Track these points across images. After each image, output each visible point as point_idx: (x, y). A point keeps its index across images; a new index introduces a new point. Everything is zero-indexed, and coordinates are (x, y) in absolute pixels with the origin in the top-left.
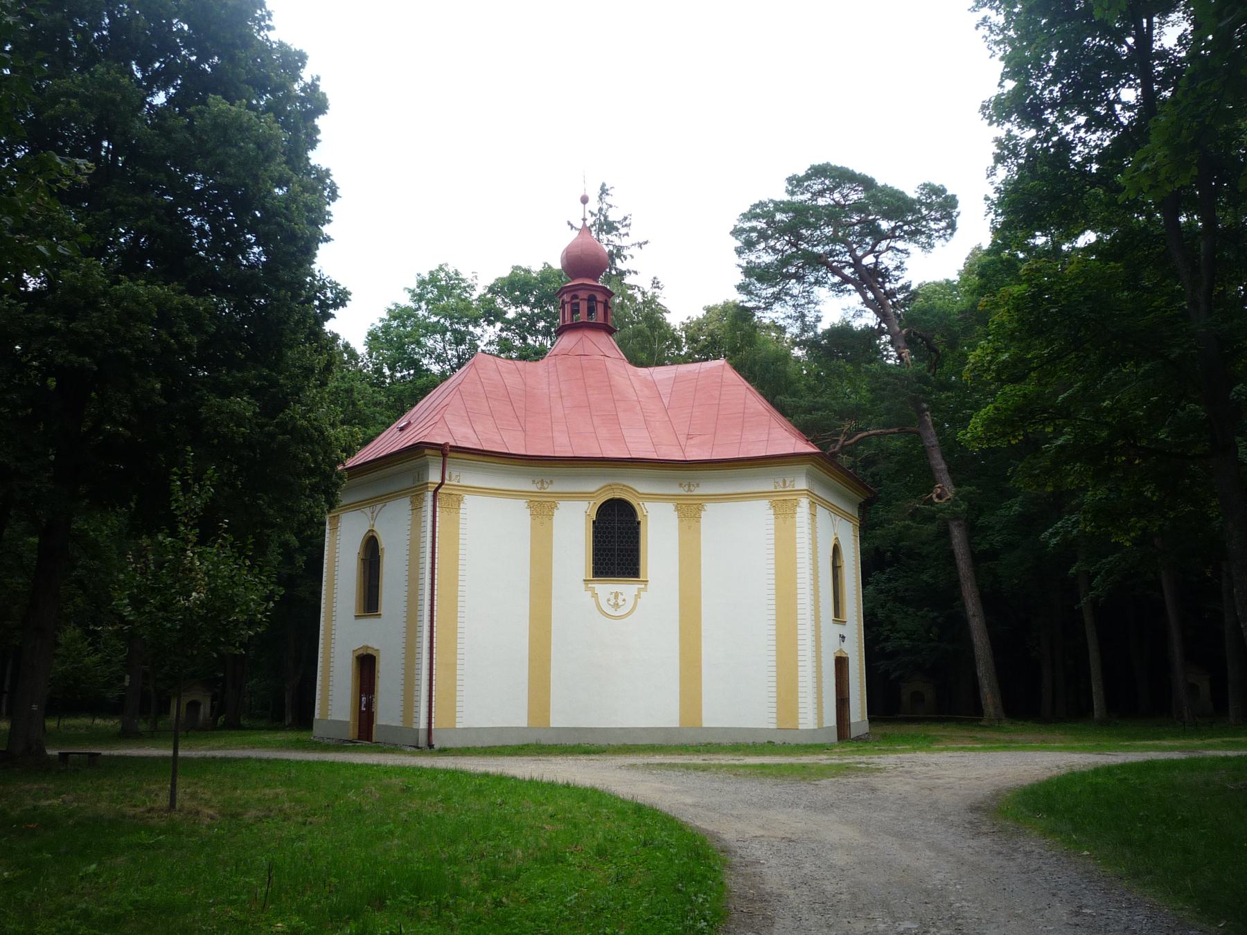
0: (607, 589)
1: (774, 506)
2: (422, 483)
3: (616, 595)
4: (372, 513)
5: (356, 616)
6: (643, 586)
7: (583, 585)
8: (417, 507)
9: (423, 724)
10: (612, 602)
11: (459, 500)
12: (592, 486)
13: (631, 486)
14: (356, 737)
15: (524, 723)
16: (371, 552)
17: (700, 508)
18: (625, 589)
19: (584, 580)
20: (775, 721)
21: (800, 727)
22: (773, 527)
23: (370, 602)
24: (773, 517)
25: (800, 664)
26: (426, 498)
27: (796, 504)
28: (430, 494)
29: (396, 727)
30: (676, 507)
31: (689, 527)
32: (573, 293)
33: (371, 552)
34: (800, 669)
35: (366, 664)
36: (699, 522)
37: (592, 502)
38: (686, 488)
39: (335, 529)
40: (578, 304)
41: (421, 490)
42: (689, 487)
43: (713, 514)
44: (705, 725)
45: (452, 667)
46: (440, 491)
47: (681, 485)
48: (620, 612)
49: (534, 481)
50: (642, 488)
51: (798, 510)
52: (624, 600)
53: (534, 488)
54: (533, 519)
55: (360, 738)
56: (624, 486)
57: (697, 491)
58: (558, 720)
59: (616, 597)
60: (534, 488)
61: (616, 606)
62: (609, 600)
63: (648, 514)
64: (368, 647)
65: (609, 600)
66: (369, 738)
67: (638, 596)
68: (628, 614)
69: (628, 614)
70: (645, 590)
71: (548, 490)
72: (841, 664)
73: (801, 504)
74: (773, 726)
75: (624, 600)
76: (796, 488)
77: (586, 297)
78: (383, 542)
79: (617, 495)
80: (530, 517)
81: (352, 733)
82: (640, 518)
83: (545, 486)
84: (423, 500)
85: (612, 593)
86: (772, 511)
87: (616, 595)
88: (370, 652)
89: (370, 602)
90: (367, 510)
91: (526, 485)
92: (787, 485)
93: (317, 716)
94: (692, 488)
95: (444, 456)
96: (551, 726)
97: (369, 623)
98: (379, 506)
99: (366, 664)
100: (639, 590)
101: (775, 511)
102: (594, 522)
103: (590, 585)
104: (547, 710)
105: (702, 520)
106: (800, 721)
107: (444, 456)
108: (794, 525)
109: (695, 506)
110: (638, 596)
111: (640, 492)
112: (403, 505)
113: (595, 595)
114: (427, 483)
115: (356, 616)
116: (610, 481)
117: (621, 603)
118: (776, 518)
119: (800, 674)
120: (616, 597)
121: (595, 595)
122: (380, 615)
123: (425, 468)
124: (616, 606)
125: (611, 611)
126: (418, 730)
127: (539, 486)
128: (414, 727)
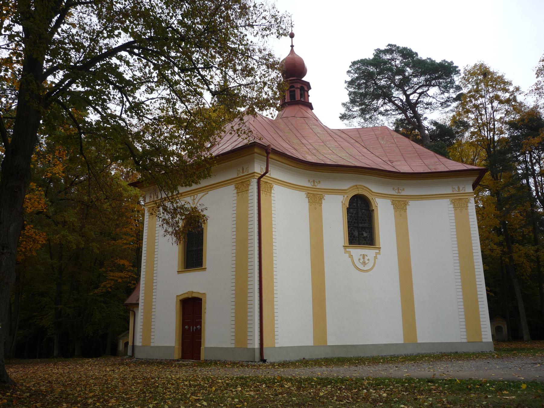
0: (357, 252)
1: (453, 202)
2: (250, 172)
3: (364, 256)
4: (194, 200)
5: (178, 272)
6: (378, 251)
7: (342, 250)
9: (257, 345)
10: (362, 261)
12: (346, 185)
13: (368, 187)
14: (180, 357)
15: (310, 342)
17: (406, 204)
18: (369, 252)
19: (344, 246)
20: (465, 337)
21: (484, 340)
22: (453, 215)
24: (453, 209)
25: (479, 300)
26: (252, 184)
27: (468, 202)
28: (254, 182)
29: (227, 348)
30: (392, 202)
31: (401, 215)
32: (291, 85)
34: (480, 303)
36: (406, 212)
37: (346, 196)
38: (397, 191)
40: (294, 91)
41: (250, 177)
42: (398, 189)
43: (413, 207)
44: (419, 341)
45: (272, 302)
46: (261, 179)
47: (393, 189)
48: (365, 268)
49: (309, 181)
50: (375, 189)
51: (469, 205)
52: (368, 260)
53: (309, 185)
54: (310, 205)
55: (184, 356)
56: (364, 187)
57: (403, 193)
58: (332, 341)
59: (364, 258)
60: (309, 185)
61: (364, 263)
62: (359, 260)
63: (378, 205)
64: (193, 292)
65: (359, 260)
66: (198, 358)
67: (376, 258)
68: (371, 269)
69: (371, 269)
70: (379, 253)
71: (317, 187)
73: (471, 201)
74: (465, 341)
75: (368, 260)
76: (466, 192)
77: (299, 87)
79: (361, 192)
80: (308, 204)
83: (316, 184)
84: (248, 185)
85: (361, 255)
86: (452, 206)
88: (195, 295)
91: (304, 182)
92: (461, 189)
94: (400, 191)
95: (268, 153)
96: (328, 344)
98: (200, 195)
100: (376, 253)
101: (454, 205)
102: (347, 208)
103: (347, 250)
104: (325, 334)
105: (408, 211)
106: (483, 336)
107: (268, 153)
108: (467, 214)
109: (403, 202)
110: (376, 258)
111: (373, 191)
112: (229, 192)
113: (351, 256)
114: (254, 173)
115: (178, 272)
116: (355, 184)
117: (367, 262)
118: (455, 210)
119: (480, 306)
120: (364, 258)
121: (351, 256)
122: (205, 268)
123: (251, 161)
124: (364, 263)
125: (361, 267)
126: (254, 349)
127: (312, 183)
128: (249, 346)
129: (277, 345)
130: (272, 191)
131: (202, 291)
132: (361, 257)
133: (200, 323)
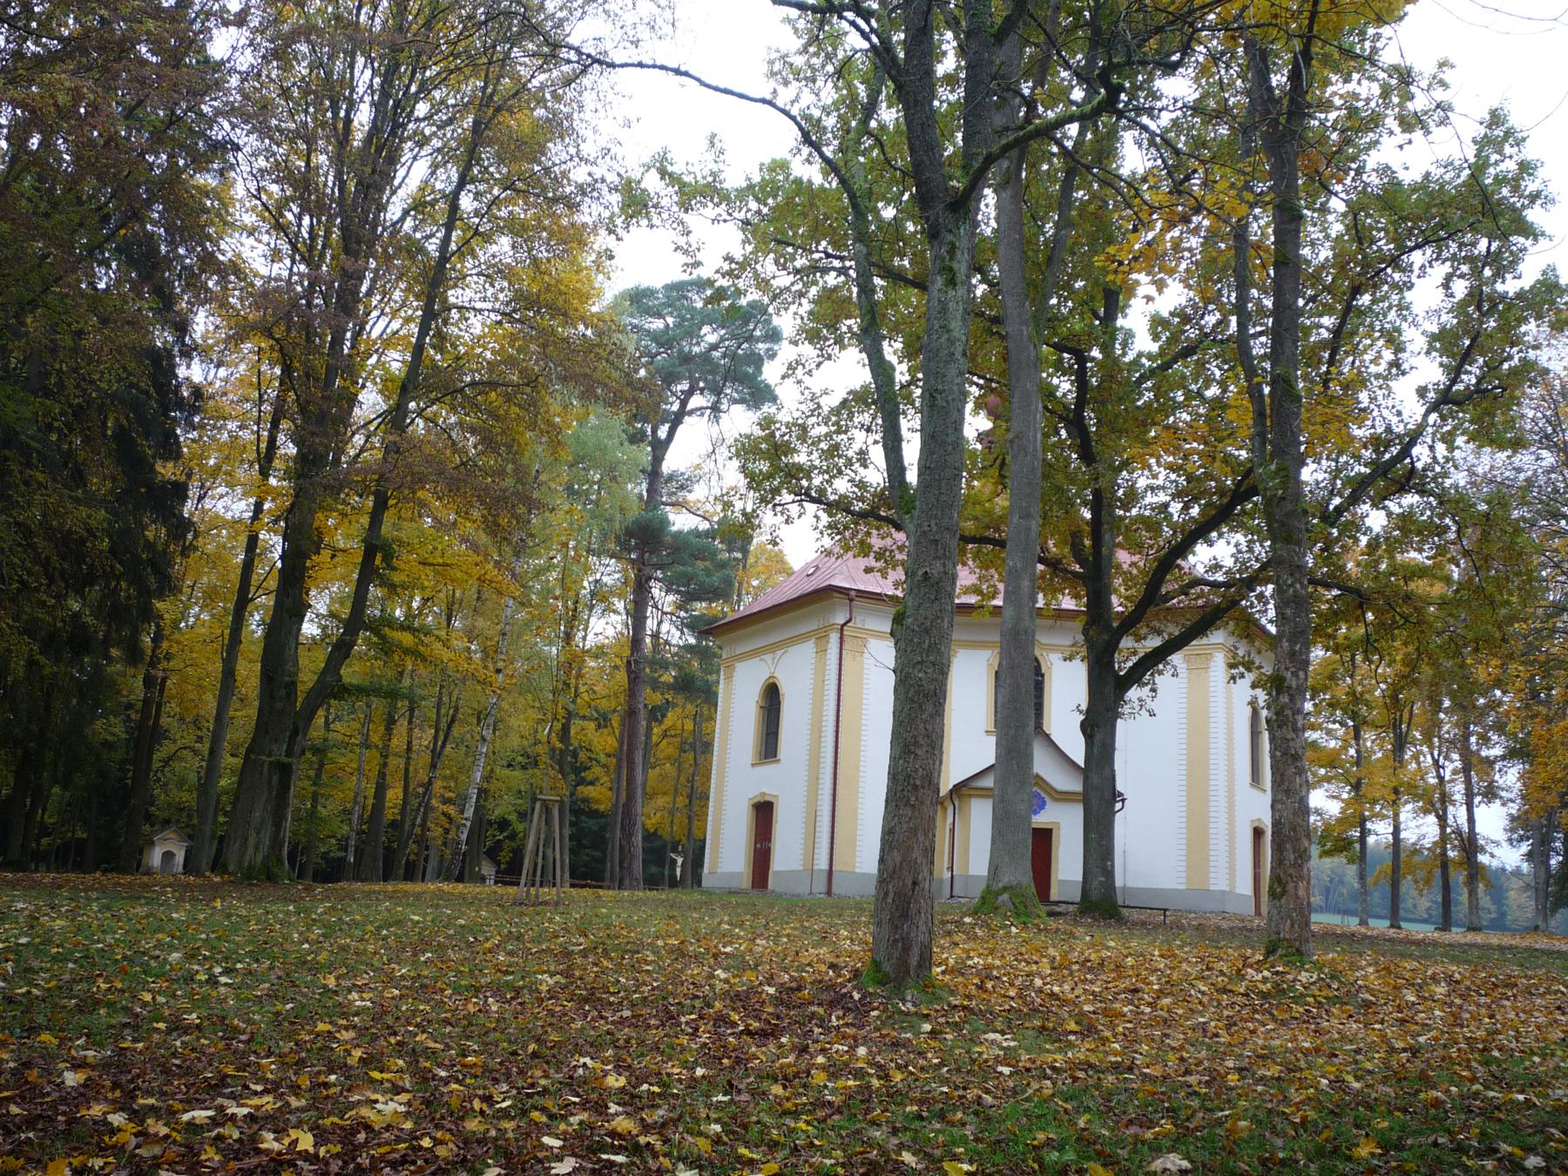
8: (822, 651)
16: (772, 696)
23: (769, 747)
33: (772, 696)
35: (764, 812)
39: (729, 678)
64: (764, 794)
78: (785, 690)
81: (746, 883)
88: (768, 798)
89: (769, 747)
90: (768, 657)
93: (706, 870)
95: (851, 600)
97: (769, 769)
98: (779, 653)
99: (764, 812)
112: (808, 648)
133: (770, 840)
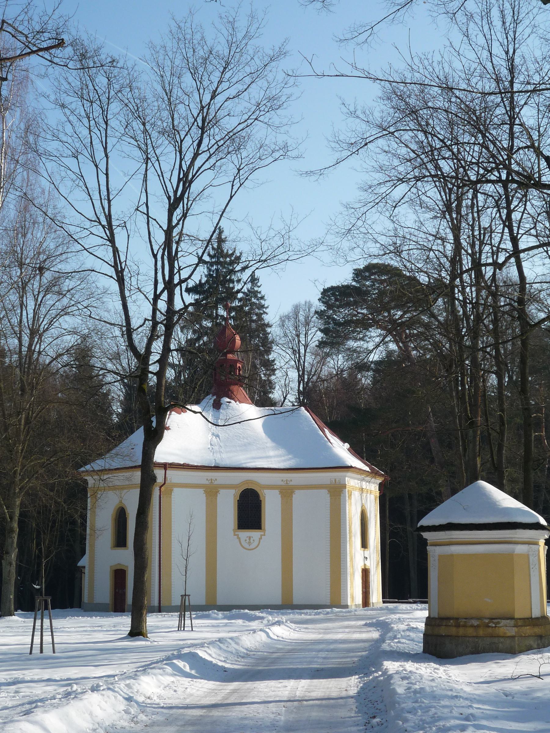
0: (245, 534)
3: (250, 538)
11: (171, 491)
17: (292, 493)
18: (254, 534)
61: (250, 543)
67: (260, 539)
72: (366, 573)
82: (261, 499)
87: (250, 538)
98: (125, 491)
100: (261, 535)
110: (260, 539)
113: (239, 539)
121: (239, 539)
124: (250, 543)
125: (247, 546)
128: (152, 605)
129: (173, 604)
130: (173, 494)
131: (126, 565)
132: (248, 539)
